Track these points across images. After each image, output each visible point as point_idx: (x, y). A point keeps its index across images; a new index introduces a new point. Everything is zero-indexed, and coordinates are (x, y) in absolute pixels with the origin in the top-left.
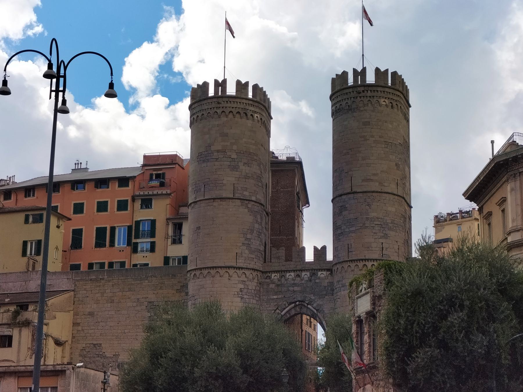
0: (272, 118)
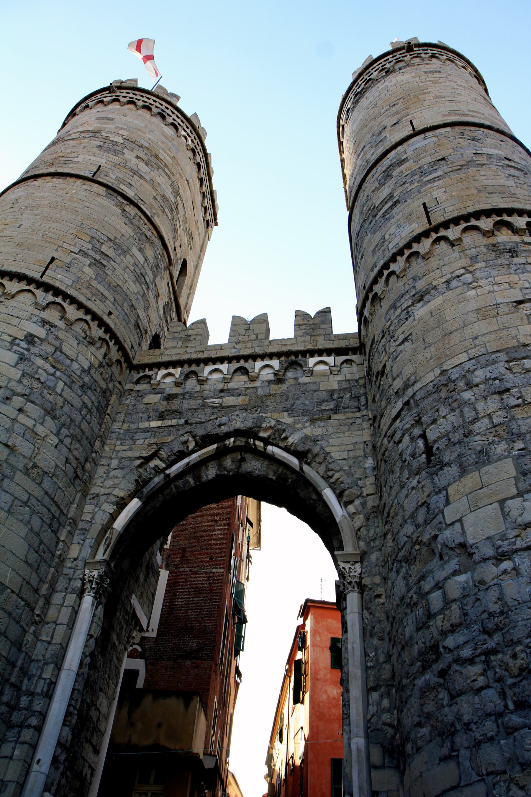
0: (216, 224)
